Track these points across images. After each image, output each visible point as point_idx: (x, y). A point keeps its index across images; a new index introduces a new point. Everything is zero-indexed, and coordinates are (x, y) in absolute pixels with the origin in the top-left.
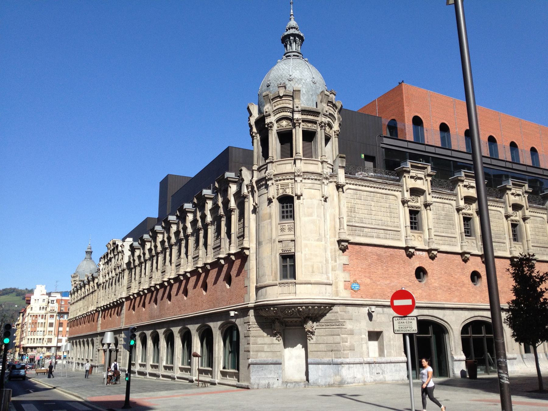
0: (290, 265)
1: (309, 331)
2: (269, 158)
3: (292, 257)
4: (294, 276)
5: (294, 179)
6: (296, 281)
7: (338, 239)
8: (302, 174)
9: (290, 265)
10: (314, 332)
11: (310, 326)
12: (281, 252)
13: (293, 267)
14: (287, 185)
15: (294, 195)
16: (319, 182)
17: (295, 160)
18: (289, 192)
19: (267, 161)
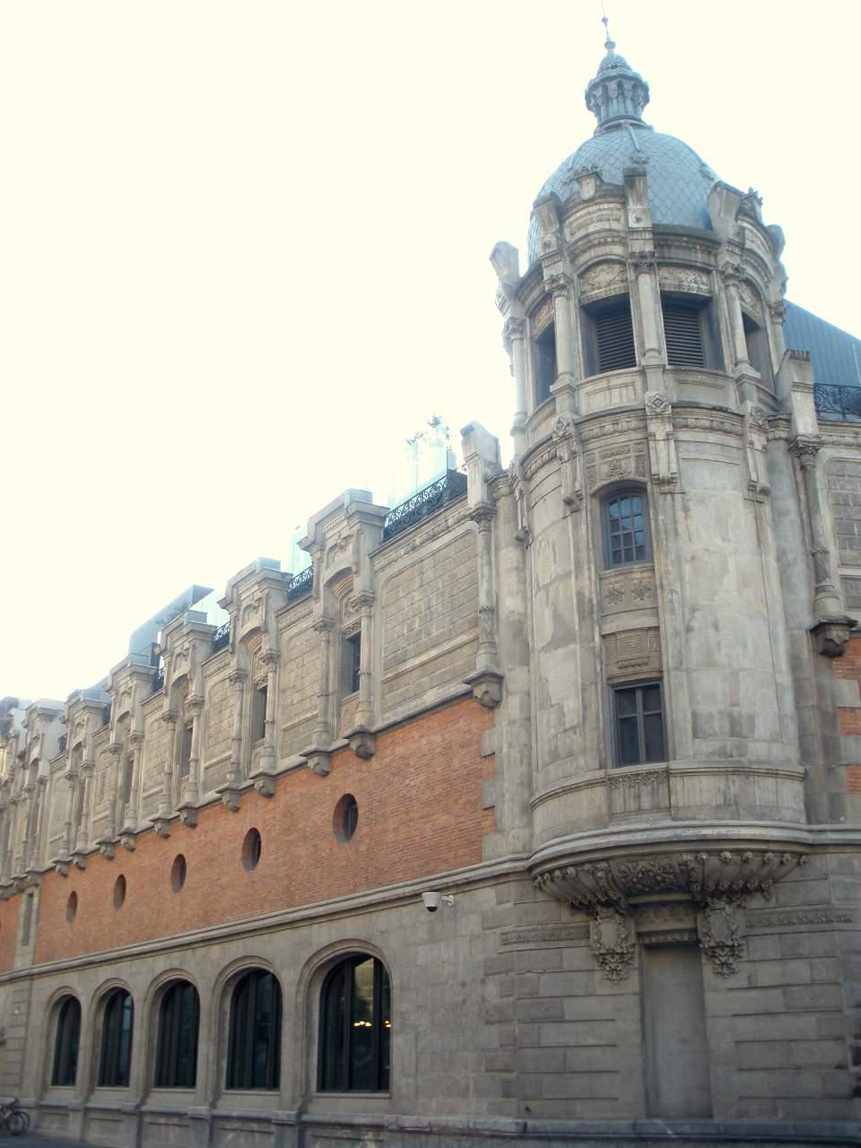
0: (645, 716)
1: (722, 946)
2: (560, 377)
3: (652, 689)
4: (658, 748)
5: (646, 428)
6: (674, 765)
7: (808, 621)
8: (669, 410)
9: (645, 716)
10: (739, 945)
11: (720, 922)
12: (615, 671)
13: (657, 721)
14: (624, 450)
15: (646, 479)
16: (733, 441)
17: (643, 372)
18: (630, 469)
19: (552, 388)
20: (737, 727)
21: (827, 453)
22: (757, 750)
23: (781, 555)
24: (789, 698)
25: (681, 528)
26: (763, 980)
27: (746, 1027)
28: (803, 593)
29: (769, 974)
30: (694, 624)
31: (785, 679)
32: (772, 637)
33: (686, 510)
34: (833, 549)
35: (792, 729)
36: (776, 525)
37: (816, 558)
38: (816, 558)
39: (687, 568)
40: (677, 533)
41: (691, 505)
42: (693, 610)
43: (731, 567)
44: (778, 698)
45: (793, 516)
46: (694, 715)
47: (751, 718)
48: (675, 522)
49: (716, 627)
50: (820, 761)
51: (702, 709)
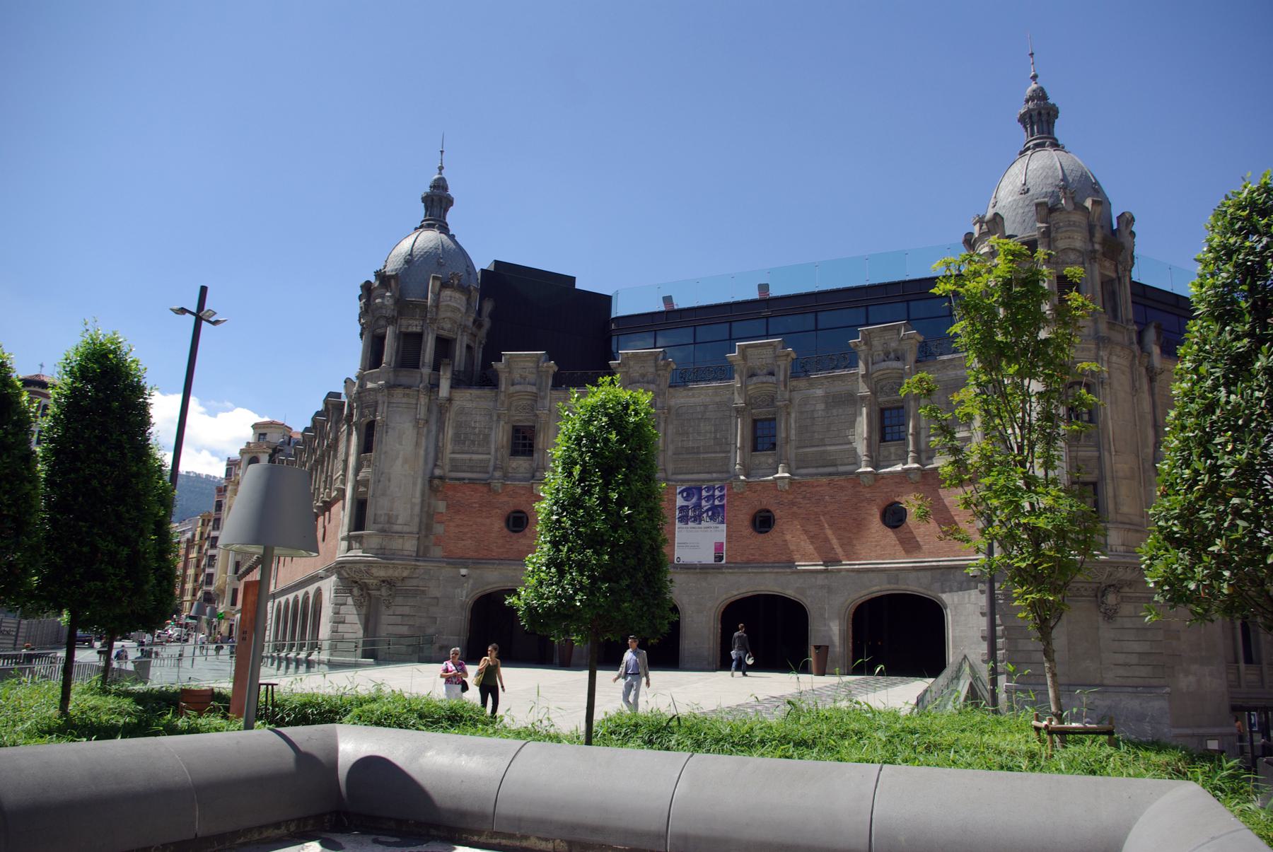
20: (391, 520)
21: (457, 404)
22: (397, 528)
23: (426, 450)
24: (417, 510)
25: (384, 441)
26: (397, 613)
27: (392, 629)
28: (430, 465)
29: (399, 610)
30: (382, 479)
31: (417, 500)
32: (415, 484)
33: (387, 432)
34: (449, 447)
35: (417, 520)
36: (427, 438)
37: (438, 451)
38: (438, 451)
39: (383, 456)
40: (382, 442)
41: (389, 430)
42: (382, 474)
43: (401, 456)
44: (412, 509)
45: (434, 432)
46: (375, 515)
47: (397, 517)
48: (382, 437)
49: (389, 481)
50: (423, 533)
51: (379, 512)
